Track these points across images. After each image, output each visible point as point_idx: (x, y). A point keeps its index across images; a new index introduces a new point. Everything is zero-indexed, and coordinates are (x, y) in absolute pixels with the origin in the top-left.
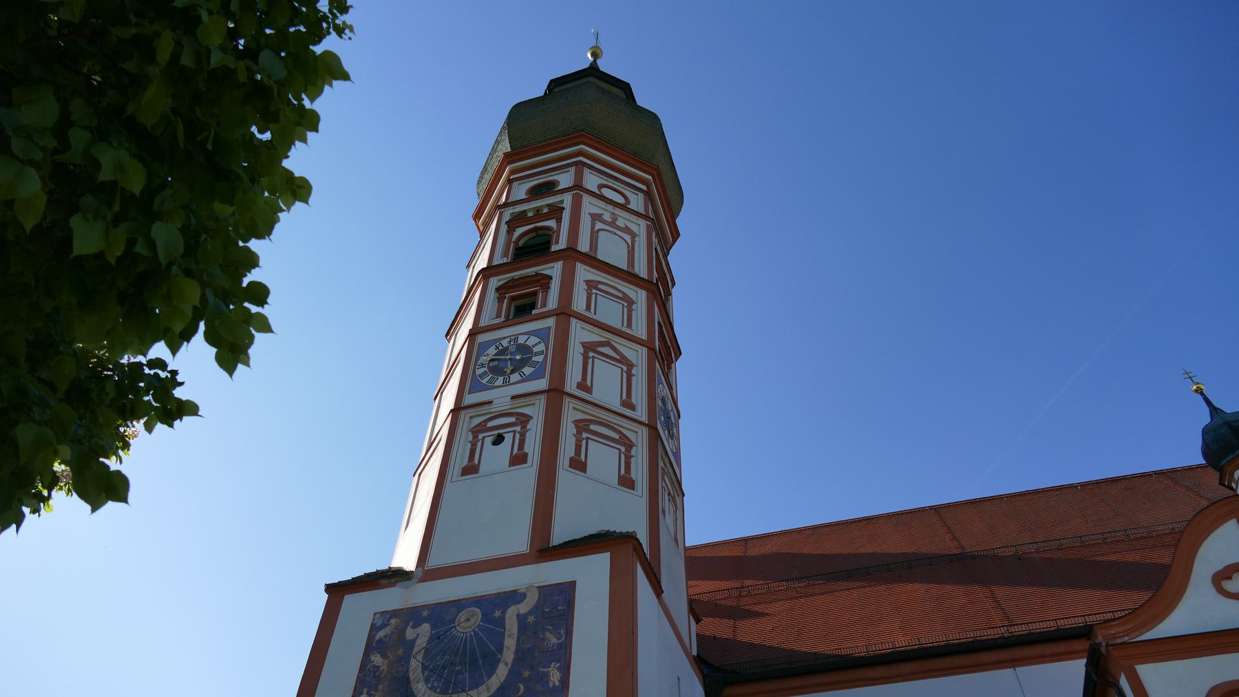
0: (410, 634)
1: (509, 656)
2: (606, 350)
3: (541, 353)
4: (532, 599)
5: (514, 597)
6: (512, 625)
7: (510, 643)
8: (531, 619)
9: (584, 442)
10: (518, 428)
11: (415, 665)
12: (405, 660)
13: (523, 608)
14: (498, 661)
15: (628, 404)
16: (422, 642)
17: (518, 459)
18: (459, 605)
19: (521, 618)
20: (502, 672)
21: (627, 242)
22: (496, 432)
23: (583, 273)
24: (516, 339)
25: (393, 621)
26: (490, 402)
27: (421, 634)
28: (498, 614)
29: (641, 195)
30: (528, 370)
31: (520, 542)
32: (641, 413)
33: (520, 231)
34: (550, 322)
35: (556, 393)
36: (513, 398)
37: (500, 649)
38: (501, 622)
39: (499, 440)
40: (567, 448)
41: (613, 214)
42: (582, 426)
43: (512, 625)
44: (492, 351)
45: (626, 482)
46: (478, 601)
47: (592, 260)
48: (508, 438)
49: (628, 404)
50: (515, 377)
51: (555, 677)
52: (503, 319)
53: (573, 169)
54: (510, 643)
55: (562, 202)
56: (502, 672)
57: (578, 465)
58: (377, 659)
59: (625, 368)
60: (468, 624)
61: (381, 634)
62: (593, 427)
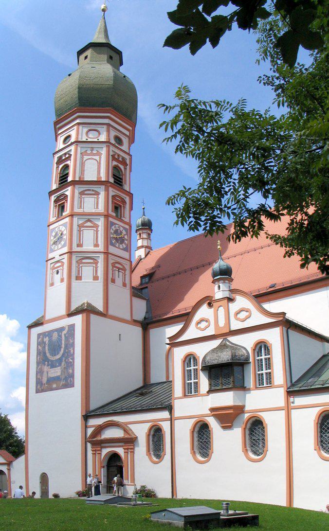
0: (45, 340)
1: (63, 346)
2: (89, 224)
3: (65, 234)
4: (67, 329)
5: (62, 329)
6: (63, 336)
7: (63, 342)
8: (67, 335)
9: (81, 268)
10: (61, 268)
11: (47, 348)
12: (45, 347)
13: (65, 332)
14: (61, 347)
15: (96, 245)
16: (47, 342)
17: (62, 280)
18: (53, 331)
19: (65, 335)
20: (62, 350)
21: (98, 161)
22: (56, 270)
23: (78, 189)
24: (59, 228)
25: (41, 336)
26: (54, 258)
27: (46, 340)
28: (60, 334)
29: (105, 127)
30: (63, 243)
31: (63, 312)
32: (101, 248)
33: (61, 166)
34: (67, 220)
35: (70, 253)
36: (60, 255)
37: (61, 344)
38: (61, 336)
39: (58, 272)
40: (74, 274)
41: (92, 147)
42: (79, 262)
43: (63, 336)
44: (54, 234)
45: (96, 278)
46: (56, 330)
47: (81, 182)
48: (60, 271)
49: (96, 245)
50: (60, 246)
51: (72, 351)
52: (55, 218)
53: (75, 127)
54: (63, 342)
55: (71, 150)
56: (62, 350)
57: (79, 278)
58: (40, 347)
59: (95, 229)
60: (55, 336)
61: (40, 340)
62: (84, 261)
